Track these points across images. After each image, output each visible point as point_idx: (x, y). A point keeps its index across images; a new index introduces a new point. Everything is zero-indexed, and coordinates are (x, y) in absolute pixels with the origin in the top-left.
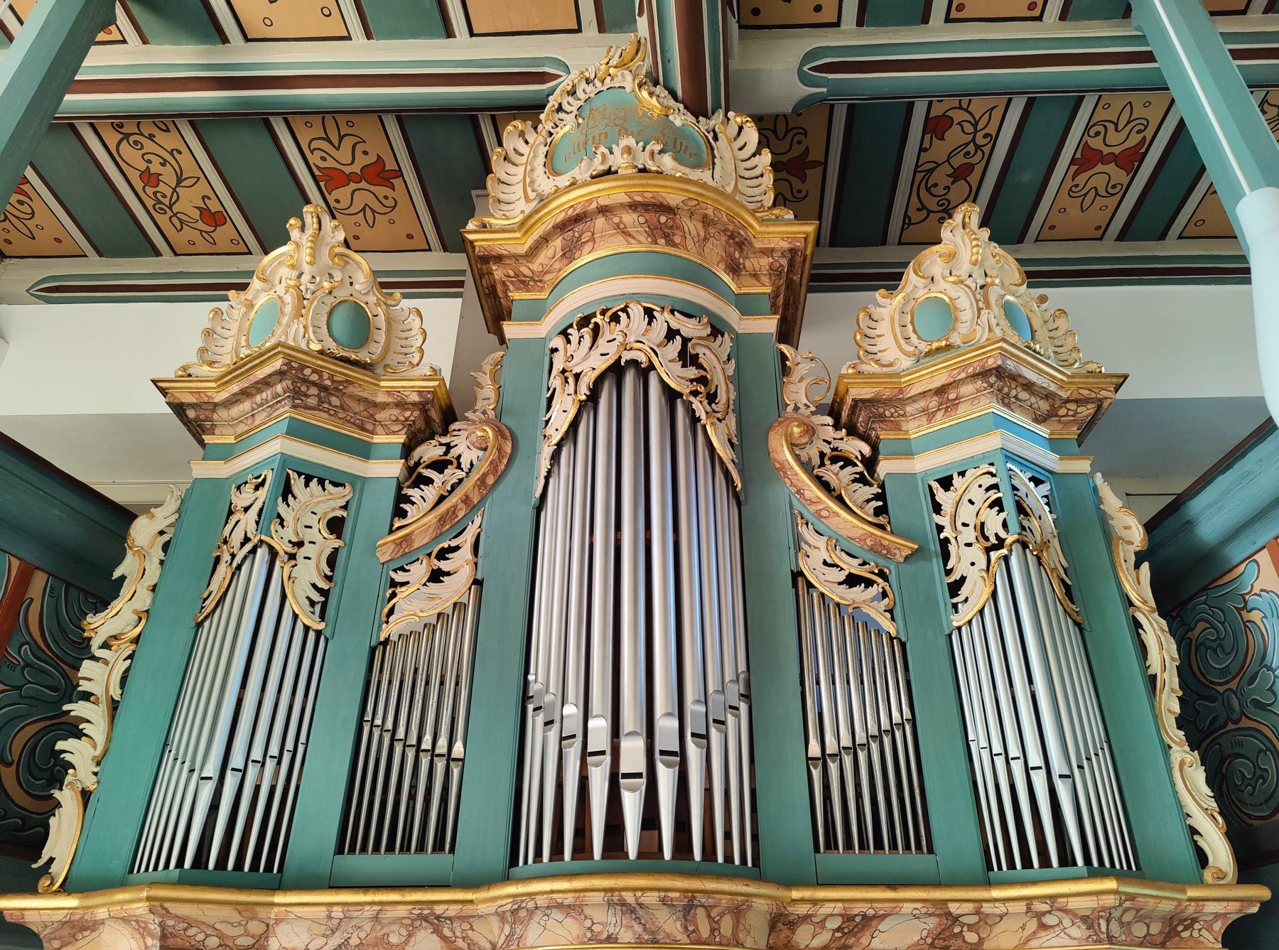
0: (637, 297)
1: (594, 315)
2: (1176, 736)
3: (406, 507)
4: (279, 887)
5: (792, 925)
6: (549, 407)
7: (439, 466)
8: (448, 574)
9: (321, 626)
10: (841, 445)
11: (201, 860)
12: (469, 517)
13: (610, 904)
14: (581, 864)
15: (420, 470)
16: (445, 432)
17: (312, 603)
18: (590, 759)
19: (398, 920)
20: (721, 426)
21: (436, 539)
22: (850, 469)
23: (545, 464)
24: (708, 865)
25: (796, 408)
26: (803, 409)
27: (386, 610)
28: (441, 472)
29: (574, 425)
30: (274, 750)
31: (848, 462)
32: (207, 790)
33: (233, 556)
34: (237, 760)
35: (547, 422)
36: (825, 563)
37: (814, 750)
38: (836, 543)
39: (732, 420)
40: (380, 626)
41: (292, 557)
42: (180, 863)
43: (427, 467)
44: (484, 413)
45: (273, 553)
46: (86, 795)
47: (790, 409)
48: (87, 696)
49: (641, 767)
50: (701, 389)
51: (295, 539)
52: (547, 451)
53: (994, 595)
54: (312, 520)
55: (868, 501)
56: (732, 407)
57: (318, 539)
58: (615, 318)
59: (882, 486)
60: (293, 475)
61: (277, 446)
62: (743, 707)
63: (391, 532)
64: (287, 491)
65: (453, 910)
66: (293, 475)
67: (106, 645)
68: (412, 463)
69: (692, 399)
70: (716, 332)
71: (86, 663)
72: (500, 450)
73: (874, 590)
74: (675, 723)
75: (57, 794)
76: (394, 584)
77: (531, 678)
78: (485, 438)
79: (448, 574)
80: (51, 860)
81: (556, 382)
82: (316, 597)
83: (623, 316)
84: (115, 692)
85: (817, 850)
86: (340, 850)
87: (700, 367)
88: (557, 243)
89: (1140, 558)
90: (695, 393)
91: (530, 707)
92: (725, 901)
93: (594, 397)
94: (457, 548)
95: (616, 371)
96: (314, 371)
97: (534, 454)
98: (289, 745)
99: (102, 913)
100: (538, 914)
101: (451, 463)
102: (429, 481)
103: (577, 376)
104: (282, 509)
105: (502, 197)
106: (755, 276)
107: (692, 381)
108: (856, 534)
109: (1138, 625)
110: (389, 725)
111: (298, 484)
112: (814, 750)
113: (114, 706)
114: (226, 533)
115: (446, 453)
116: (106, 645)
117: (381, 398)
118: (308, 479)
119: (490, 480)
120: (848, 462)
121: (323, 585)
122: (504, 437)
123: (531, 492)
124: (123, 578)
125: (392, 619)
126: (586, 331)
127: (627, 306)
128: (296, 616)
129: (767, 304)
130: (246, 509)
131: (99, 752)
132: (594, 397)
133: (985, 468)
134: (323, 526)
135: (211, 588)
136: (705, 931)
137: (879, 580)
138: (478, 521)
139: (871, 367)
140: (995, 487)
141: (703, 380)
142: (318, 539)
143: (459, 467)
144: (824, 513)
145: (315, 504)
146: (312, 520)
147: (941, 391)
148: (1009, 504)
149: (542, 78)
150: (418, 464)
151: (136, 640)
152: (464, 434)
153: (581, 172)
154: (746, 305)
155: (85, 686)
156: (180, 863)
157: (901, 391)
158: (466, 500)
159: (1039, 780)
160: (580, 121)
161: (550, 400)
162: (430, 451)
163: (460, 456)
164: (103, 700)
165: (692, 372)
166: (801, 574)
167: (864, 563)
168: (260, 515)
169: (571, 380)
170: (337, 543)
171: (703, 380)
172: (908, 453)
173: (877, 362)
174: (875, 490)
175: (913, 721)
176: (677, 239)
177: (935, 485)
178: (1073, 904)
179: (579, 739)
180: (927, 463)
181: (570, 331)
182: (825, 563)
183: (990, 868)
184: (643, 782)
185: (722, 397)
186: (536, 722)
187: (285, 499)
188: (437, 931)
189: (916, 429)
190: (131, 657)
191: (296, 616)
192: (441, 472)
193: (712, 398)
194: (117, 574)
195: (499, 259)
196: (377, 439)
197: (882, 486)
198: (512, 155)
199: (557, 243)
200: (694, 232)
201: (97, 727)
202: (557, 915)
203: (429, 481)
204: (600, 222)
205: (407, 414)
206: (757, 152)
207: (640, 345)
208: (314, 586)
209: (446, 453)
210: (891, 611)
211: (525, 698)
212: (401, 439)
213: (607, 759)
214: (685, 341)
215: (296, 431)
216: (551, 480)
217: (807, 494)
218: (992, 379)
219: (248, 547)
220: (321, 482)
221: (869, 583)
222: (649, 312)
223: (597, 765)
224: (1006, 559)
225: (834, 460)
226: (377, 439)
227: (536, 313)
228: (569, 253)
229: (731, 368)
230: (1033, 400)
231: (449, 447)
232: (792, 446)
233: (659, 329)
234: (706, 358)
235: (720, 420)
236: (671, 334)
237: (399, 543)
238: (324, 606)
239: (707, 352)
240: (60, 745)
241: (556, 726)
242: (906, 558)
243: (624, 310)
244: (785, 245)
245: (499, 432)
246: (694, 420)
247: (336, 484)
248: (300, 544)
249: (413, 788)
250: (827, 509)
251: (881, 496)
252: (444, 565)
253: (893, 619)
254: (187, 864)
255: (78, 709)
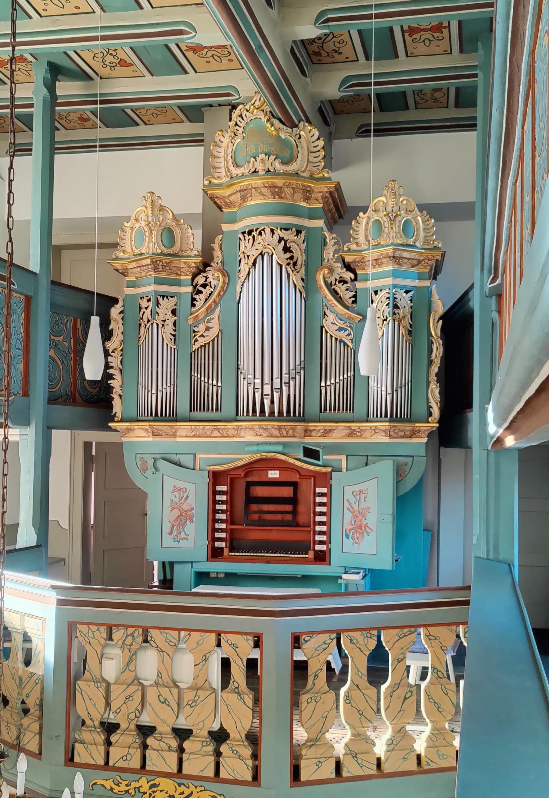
0: (268, 224)
1: (252, 231)
2: (433, 378)
3: (195, 302)
4: (176, 421)
5: (311, 431)
6: (240, 265)
7: (204, 286)
8: (211, 328)
9: (175, 347)
10: (343, 275)
11: (156, 414)
12: (216, 307)
13: (260, 428)
14: (254, 418)
15: (197, 287)
16: (204, 271)
17: (171, 340)
18: (255, 390)
19: (209, 429)
20: (299, 275)
21: (207, 315)
22: (345, 285)
23: (239, 290)
24: (288, 418)
25: (328, 260)
26: (330, 261)
27: (193, 341)
28: (205, 288)
29: (249, 274)
30: (169, 385)
31: (345, 282)
32: (154, 397)
33: (146, 326)
34: (160, 388)
35: (240, 270)
36: (332, 323)
37: (323, 384)
38: (337, 315)
39: (303, 270)
40: (192, 347)
41: (163, 325)
42: (151, 415)
43: (201, 286)
44: (217, 263)
45: (157, 325)
46: (120, 396)
47: (326, 261)
48: (112, 367)
49: (269, 393)
50: (291, 262)
51: (163, 319)
52: (239, 284)
53: (383, 335)
54: (167, 312)
55: (350, 298)
56: (304, 263)
57: (170, 318)
58: (260, 234)
59: (356, 292)
60: (159, 297)
61: (151, 288)
62: (302, 372)
63: (191, 314)
64: (158, 304)
65: (222, 427)
66: (159, 297)
67: (113, 352)
68: (194, 284)
69: (287, 267)
70: (298, 232)
71: (109, 357)
72: (224, 281)
73: (347, 332)
74: (279, 380)
75: (112, 395)
76: (194, 332)
77: (239, 363)
78: (218, 277)
79: (211, 328)
80: (116, 413)
81: (242, 256)
82: (173, 338)
83: (263, 232)
84: (120, 367)
85: (321, 411)
86: (191, 411)
87: (291, 252)
88: (239, 194)
89: (440, 318)
90: (288, 264)
91: (239, 372)
92: (289, 427)
93: (255, 261)
94: (213, 318)
95: (261, 254)
96: (160, 261)
97: (236, 283)
98: (172, 383)
99: (136, 427)
100: (243, 430)
101: (208, 285)
102: (201, 292)
103: (248, 256)
104: (157, 310)
105: (217, 165)
106: (317, 200)
107: (287, 259)
108: (343, 313)
109: (432, 343)
110: (199, 376)
111: (160, 299)
112: (323, 384)
113: (121, 370)
114: (141, 315)
115: (206, 281)
116: (113, 352)
117: (182, 265)
118: (163, 297)
119: (222, 293)
120: (345, 282)
121: (173, 333)
122: (225, 276)
123: (236, 299)
124: (112, 329)
125: (196, 343)
126: (250, 237)
127: (264, 228)
128: (167, 344)
129: (321, 213)
130: (146, 308)
131: (120, 383)
132: (255, 261)
133: (387, 291)
134: (170, 313)
135: (141, 334)
136: (285, 434)
137: (349, 329)
138: (219, 308)
139: (354, 247)
140: (388, 298)
141: (291, 258)
142: (170, 318)
143: (211, 287)
144: (333, 305)
145: (167, 305)
146: (167, 312)
147: (376, 260)
148: (391, 305)
149: (228, 95)
150: (197, 285)
151: (122, 350)
152: (211, 273)
153: (245, 170)
154: (312, 215)
155: (111, 364)
156: (151, 415)
157: (363, 258)
158: (214, 301)
159: (384, 393)
160: (244, 135)
161: (240, 261)
162: (200, 280)
163: (210, 282)
164: (117, 368)
165: (288, 255)
166: (324, 326)
167: (345, 323)
168: (151, 312)
169: (246, 257)
170: (176, 318)
171: (291, 258)
172: (367, 280)
173: (357, 244)
174: (354, 293)
175: (354, 375)
176: (283, 195)
177: (373, 293)
178: (380, 428)
179: (253, 384)
180: (371, 284)
181: (245, 235)
182: (332, 323)
183: (368, 416)
184: (270, 397)
185: (299, 263)
186: (241, 377)
187: (158, 306)
188: (218, 431)
189: (370, 271)
190: (121, 355)
191: (167, 344)
192: (205, 288)
193: (295, 264)
194: (110, 328)
195: (217, 197)
196: (182, 277)
197: (356, 292)
198: (219, 142)
199: (239, 194)
200: (289, 192)
201: (118, 376)
202: (247, 429)
203: (201, 292)
204: (253, 190)
205: (191, 269)
206: (319, 139)
207: (269, 246)
208: (171, 334)
209: (206, 281)
210: (352, 340)
211: (238, 368)
212: (190, 277)
213: (260, 390)
214: (286, 241)
215: (158, 282)
216: (242, 294)
217: (328, 298)
218: (392, 259)
219: (150, 323)
220: (167, 297)
221: (346, 330)
222: (272, 231)
223: (257, 392)
224: (388, 324)
225: (339, 282)
226: (182, 277)
227: (234, 222)
228: (244, 199)
229: (304, 246)
230: (410, 261)
231: (207, 278)
232: (324, 278)
233: (276, 237)
234: (294, 247)
235: (298, 272)
236: (281, 239)
237: (194, 318)
238: (175, 340)
239: (293, 244)
240: (109, 382)
241: (246, 379)
242: (359, 321)
243: (263, 230)
244: (326, 190)
245: (223, 275)
246: (289, 275)
247: (172, 297)
248: (165, 321)
249: (208, 393)
250: (334, 303)
251: (355, 296)
252: (210, 325)
253: (352, 342)
254: (154, 415)
255: (111, 371)
